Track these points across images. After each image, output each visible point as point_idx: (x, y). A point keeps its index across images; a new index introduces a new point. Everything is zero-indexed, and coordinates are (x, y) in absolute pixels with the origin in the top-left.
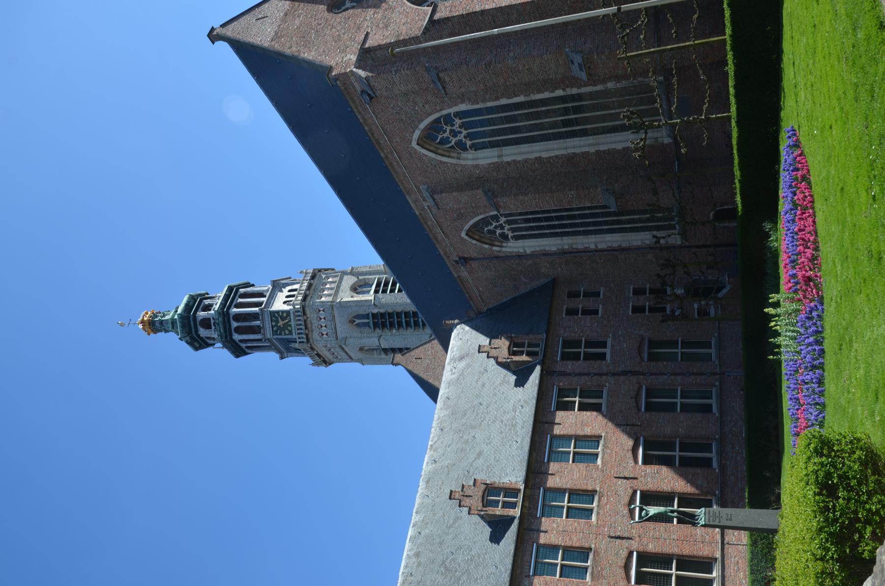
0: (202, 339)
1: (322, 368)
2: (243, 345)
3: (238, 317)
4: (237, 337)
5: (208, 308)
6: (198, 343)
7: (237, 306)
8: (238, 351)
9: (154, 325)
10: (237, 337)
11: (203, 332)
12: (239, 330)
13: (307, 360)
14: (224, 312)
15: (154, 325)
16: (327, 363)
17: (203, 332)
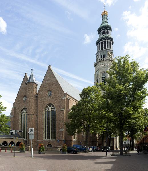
0: (100, 32)
1: (94, 65)
2: (98, 44)
3: (105, 42)
4: (100, 43)
5: (108, 33)
6: (99, 31)
7: (108, 41)
8: (97, 43)
9: (104, 15)
10: (100, 43)
11: (101, 32)
12: (102, 43)
13: (95, 62)
14: (107, 38)
15: (104, 15)
16: (95, 66)
17: (101, 32)
